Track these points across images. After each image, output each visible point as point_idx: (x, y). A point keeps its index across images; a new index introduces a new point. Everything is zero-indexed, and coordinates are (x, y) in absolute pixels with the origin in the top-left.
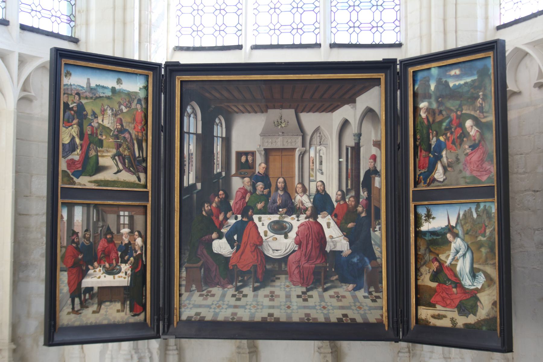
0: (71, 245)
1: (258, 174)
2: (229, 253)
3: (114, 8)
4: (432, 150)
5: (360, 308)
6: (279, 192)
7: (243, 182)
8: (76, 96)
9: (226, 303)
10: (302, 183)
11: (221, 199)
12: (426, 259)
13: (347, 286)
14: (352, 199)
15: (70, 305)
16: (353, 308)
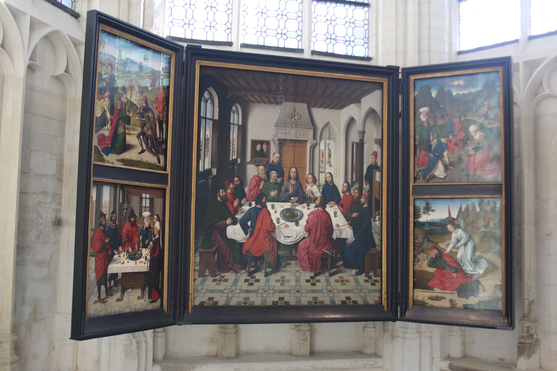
0: (99, 227)
1: (272, 163)
2: (242, 239)
4: (432, 150)
5: (361, 291)
6: (292, 181)
7: (258, 170)
8: (109, 67)
9: (239, 288)
10: (312, 173)
11: (236, 185)
12: (424, 246)
13: (351, 271)
14: (356, 191)
15: (96, 293)
16: (355, 291)
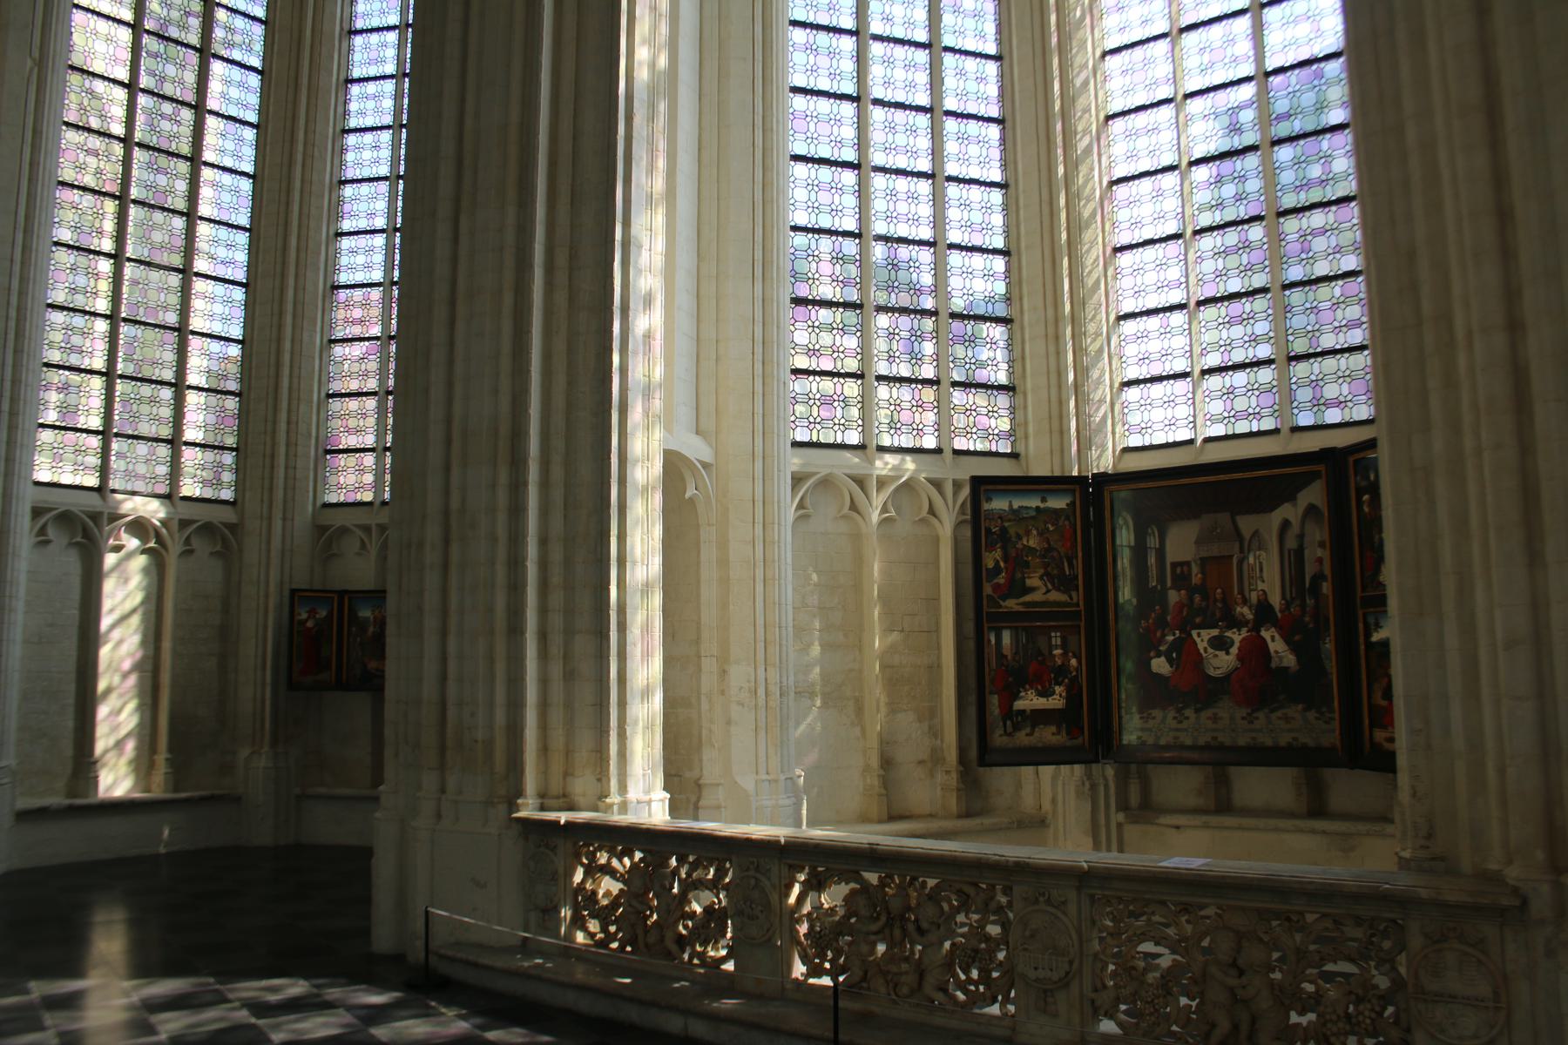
3: (1050, 418)
10: (1241, 592)
14: (1297, 608)
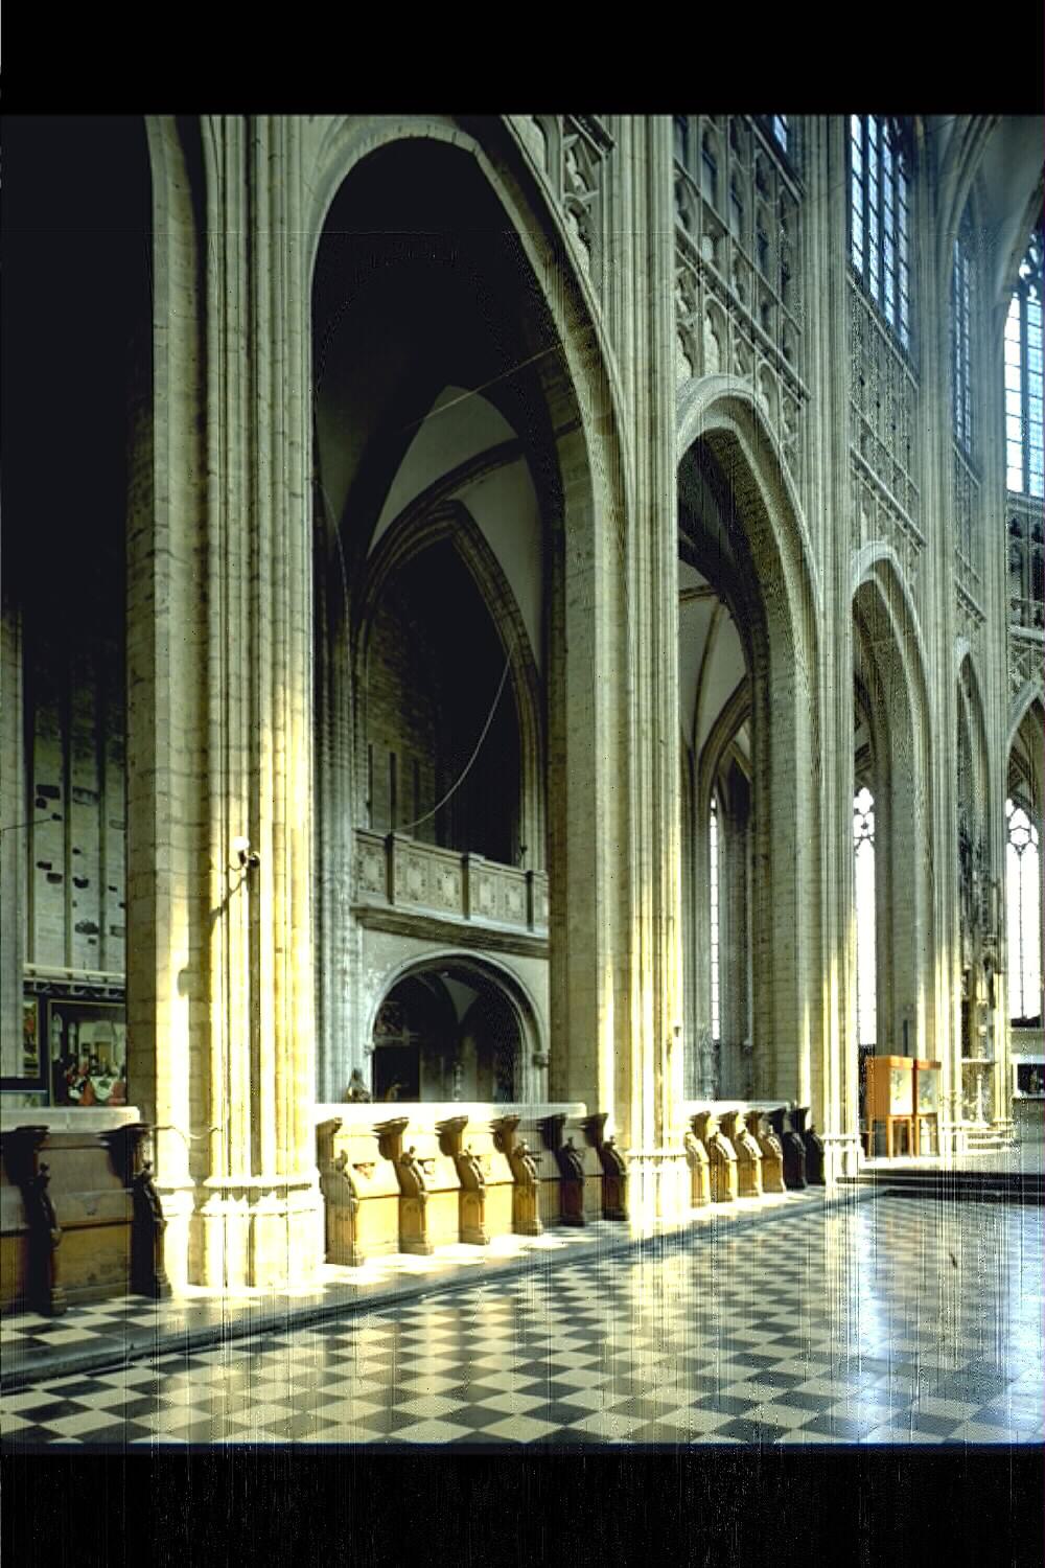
10: (115, 1060)
